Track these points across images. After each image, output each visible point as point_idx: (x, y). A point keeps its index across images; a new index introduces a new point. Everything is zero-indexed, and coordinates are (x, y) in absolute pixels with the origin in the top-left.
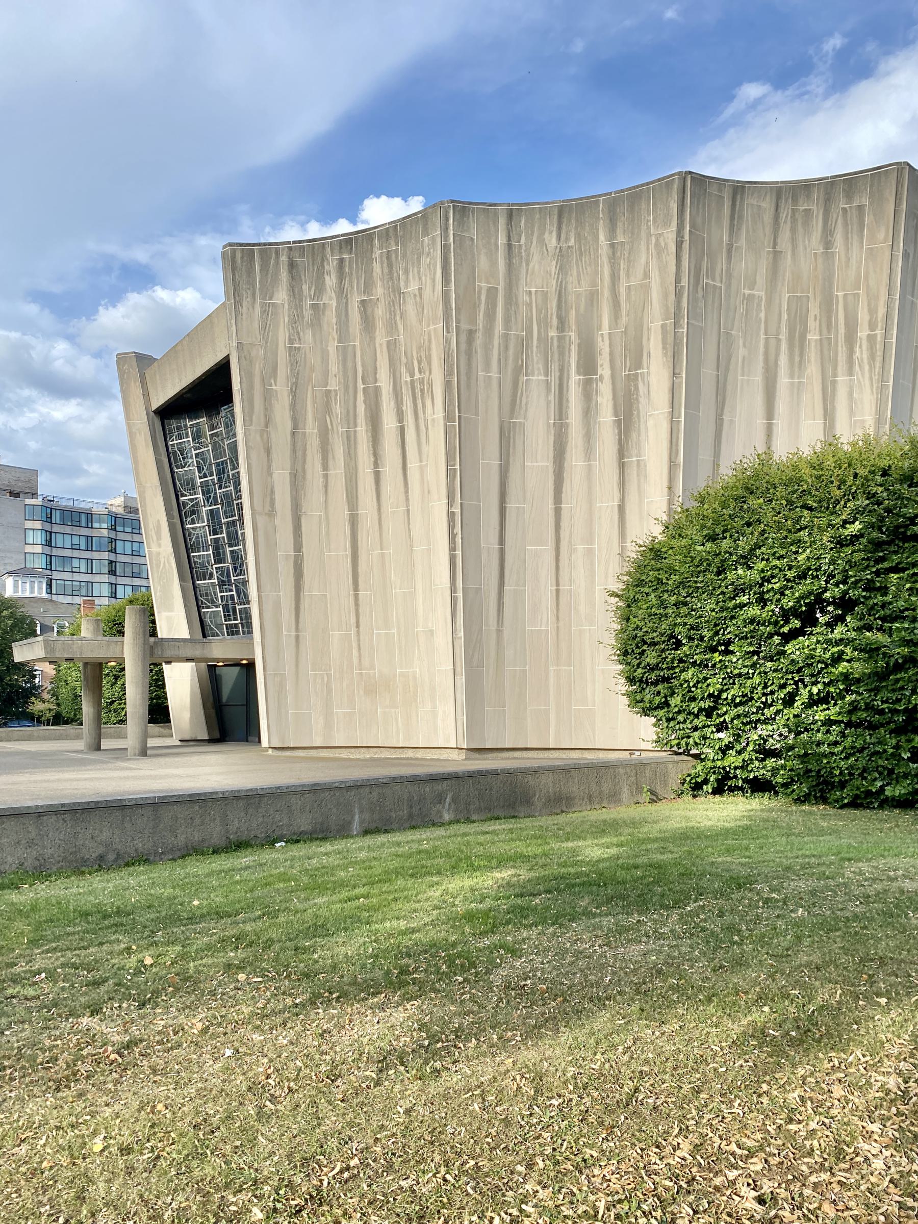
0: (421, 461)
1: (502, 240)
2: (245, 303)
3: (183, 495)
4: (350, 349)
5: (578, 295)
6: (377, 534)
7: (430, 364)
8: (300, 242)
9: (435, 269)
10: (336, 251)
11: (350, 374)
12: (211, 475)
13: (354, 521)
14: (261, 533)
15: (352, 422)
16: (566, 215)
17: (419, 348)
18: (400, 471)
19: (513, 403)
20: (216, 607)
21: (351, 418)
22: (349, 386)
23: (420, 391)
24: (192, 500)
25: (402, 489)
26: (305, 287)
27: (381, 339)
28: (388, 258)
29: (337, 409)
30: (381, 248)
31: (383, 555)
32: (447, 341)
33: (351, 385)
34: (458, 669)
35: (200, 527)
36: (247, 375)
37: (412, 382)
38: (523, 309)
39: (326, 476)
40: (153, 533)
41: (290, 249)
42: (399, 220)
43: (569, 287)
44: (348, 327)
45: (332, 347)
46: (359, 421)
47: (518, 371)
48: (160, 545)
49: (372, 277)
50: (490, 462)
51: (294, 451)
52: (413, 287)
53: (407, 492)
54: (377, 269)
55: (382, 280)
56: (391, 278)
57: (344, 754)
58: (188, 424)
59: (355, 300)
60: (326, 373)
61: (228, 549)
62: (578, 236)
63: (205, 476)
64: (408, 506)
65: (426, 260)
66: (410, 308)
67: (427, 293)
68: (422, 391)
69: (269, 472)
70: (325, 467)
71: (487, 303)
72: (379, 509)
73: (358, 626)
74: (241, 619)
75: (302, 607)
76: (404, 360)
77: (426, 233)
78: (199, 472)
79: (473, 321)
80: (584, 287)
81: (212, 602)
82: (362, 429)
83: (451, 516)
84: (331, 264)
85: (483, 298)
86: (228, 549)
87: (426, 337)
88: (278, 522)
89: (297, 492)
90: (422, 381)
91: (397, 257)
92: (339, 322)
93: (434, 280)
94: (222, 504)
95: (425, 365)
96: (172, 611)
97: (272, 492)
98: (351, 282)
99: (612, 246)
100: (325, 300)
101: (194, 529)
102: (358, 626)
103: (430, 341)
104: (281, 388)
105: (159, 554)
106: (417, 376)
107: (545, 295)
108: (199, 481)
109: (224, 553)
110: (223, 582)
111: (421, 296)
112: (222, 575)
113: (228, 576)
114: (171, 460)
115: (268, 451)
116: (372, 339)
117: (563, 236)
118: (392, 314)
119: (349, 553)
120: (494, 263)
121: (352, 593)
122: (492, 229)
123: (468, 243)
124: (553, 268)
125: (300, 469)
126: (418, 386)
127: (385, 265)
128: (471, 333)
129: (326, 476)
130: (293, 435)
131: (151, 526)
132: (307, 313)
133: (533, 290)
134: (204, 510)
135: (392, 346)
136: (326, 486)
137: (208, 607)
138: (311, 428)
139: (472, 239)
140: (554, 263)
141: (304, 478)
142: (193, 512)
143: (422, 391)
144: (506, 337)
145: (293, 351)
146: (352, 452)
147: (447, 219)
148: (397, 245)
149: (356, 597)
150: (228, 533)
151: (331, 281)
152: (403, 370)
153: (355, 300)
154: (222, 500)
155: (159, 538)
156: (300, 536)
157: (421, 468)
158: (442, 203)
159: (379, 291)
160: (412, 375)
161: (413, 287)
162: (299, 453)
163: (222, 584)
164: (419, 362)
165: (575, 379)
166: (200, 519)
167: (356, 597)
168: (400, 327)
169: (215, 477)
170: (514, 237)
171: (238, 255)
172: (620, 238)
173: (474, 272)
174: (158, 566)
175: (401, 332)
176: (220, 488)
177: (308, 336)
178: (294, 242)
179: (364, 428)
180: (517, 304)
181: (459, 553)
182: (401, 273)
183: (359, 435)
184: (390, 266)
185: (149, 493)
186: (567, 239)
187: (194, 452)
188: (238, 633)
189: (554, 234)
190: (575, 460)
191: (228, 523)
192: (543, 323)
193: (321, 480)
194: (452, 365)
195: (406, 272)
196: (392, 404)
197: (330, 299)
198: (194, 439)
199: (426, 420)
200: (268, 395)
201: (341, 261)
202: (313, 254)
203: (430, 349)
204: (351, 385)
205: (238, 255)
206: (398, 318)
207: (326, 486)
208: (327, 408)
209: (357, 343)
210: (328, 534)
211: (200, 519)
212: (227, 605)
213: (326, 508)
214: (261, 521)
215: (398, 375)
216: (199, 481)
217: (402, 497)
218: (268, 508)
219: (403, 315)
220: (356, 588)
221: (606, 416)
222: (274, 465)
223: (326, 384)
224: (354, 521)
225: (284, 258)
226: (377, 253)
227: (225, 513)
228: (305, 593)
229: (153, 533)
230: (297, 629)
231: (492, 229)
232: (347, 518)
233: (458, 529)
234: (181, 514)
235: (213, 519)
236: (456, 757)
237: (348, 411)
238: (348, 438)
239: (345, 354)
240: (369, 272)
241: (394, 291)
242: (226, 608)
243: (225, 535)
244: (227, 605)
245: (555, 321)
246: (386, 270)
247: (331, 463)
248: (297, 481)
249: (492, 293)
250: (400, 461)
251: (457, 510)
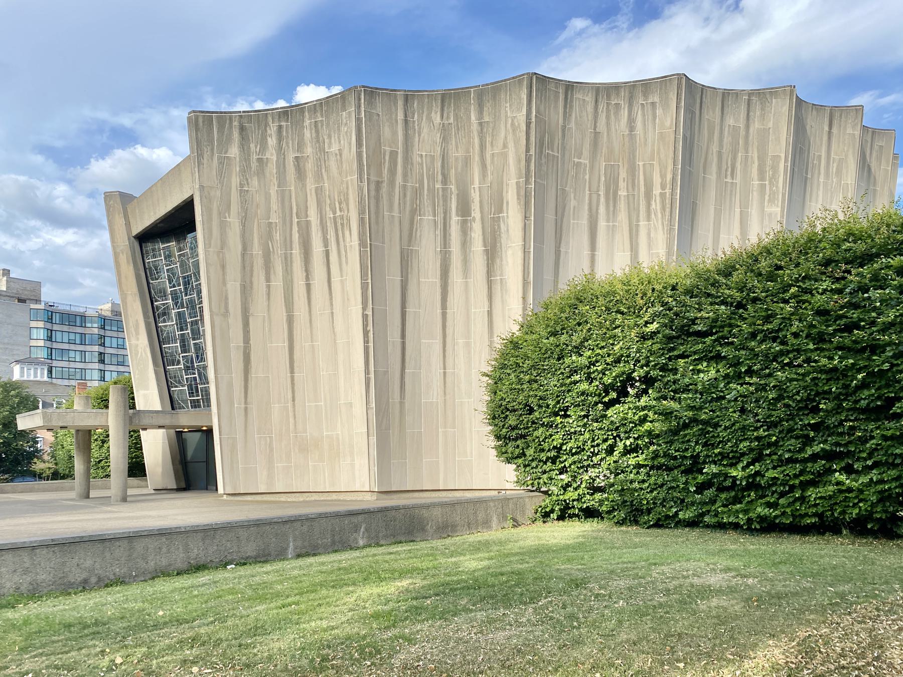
0: (342, 276)
1: (400, 116)
2: (205, 156)
3: (156, 301)
4: (287, 193)
5: (457, 159)
6: (309, 331)
7: (347, 205)
8: (248, 112)
9: (351, 136)
10: (276, 120)
11: (287, 211)
13: (290, 320)
14: (217, 329)
15: (288, 246)
16: (447, 101)
17: (339, 193)
18: (326, 284)
19: (410, 236)
20: (183, 386)
21: (287, 244)
22: (286, 221)
23: (340, 225)
24: (164, 304)
25: (327, 296)
26: (252, 146)
27: (311, 185)
28: (316, 126)
29: (277, 236)
30: (310, 118)
31: (313, 346)
32: (361, 189)
33: (288, 219)
34: (371, 432)
35: (170, 325)
36: (208, 210)
37: (335, 218)
38: (416, 168)
39: (268, 287)
40: (133, 330)
41: (241, 116)
42: (324, 99)
43: (450, 152)
44: (285, 177)
45: (273, 190)
46: (294, 246)
47: (413, 212)
48: (138, 339)
49: (303, 139)
50: (393, 278)
51: (244, 267)
52: (335, 148)
53: (331, 299)
54: (307, 134)
55: (311, 142)
56: (318, 141)
57: (283, 498)
59: (291, 156)
60: (268, 210)
61: (192, 342)
62: (456, 117)
63: (174, 286)
64: (332, 309)
65: (344, 129)
66: (333, 164)
67: (345, 152)
68: (342, 225)
69: (224, 283)
70: (268, 280)
71: (390, 162)
72: (310, 312)
73: (294, 400)
75: (249, 386)
76: (328, 202)
77: (344, 108)
78: (170, 283)
79: (380, 174)
80: (460, 154)
81: (180, 382)
82: (296, 251)
83: (365, 317)
84: (272, 129)
85: (387, 158)
86: (192, 342)
87: (345, 186)
88: (231, 320)
89: (246, 299)
90: (342, 217)
91: (322, 126)
92: (278, 172)
93: (350, 144)
94: (187, 308)
95: (344, 206)
96: (148, 389)
97: (227, 298)
98: (287, 143)
99: (481, 124)
100: (268, 155)
101: (166, 326)
102: (294, 400)
103: (347, 188)
104: (234, 220)
105: (137, 345)
106: (338, 213)
107: (433, 157)
109: (189, 345)
110: (188, 367)
111: (341, 155)
113: (192, 362)
114: (148, 273)
115: (223, 267)
116: (304, 186)
117: (445, 115)
118: (319, 167)
119: (286, 344)
120: (395, 133)
121: (289, 375)
122: (393, 108)
123: (375, 117)
124: (438, 138)
125: (248, 282)
126: (339, 221)
127: (313, 131)
128: (378, 184)
129: (268, 287)
130: (243, 255)
131: (131, 324)
132: (254, 165)
133: (424, 154)
134: (173, 312)
135: (319, 191)
136: (269, 294)
137: (176, 387)
138: (257, 250)
139: (378, 115)
140: (439, 135)
141: (251, 288)
142: (164, 314)
143: (342, 225)
144: (405, 187)
145: (243, 193)
146: (289, 268)
147: (360, 99)
148: (322, 116)
149: (292, 378)
150: (192, 330)
151: (272, 141)
152: (328, 209)
153: (291, 156)
155: (137, 333)
156: (248, 332)
157: (341, 281)
158: (356, 87)
159: (309, 150)
160: (335, 213)
161: (335, 148)
162: (248, 269)
163: (187, 368)
164: (340, 203)
165: (455, 219)
166: (170, 319)
167: (292, 378)
168: (325, 177)
170: (409, 114)
171: (200, 120)
172: (486, 119)
173: (380, 140)
174: (137, 354)
175: (326, 181)
176: (186, 295)
177: (255, 182)
178: (244, 112)
179: (298, 251)
180: (412, 164)
181: (371, 344)
182: (325, 137)
183: (294, 256)
184: (317, 132)
185: (130, 299)
186: (448, 118)
188: (199, 406)
189: (439, 114)
190: (456, 276)
191: (192, 322)
192: (432, 178)
193: (265, 289)
194: (364, 207)
195: (330, 137)
196: (320, 234)
197: (271, 155)
198: (165, 258)
199: (345, 246)
200: (223, 226)
201: (280, 127)
202: (258, 121)
203: (348, 194)
204: (288, 219)
205: (200, 120)
206: (323, 170)
207: (269, 294)
208: (270, 236)
209: (293, 188)
210: (270, 330)
211: (170, 319)
212: (191, 385)
213: (268, 310)
214: (217, 320)
215: (324, 213)
216: (169, 290)
217: (328, 303)
218: (223, 310)
220: (292, 371)
222: (228, 278)
223: (269, 218)
224: (290, 320)
225: (236, 123)
226: (307, 122)
227: (190, 314)
228: (253, 375)
229: (133, 330)
230: (246, 403)
231: (393, 108)
232: (285, 318)
233: (370, 328)
234: (156, 315)
235: (180, 319)
236: (369, 498)
237: (286, 239)
238: (286, 258)
239: (283, 196)
241: (320, 151)
244: (191, 385)
245: (440, 177)
246: (314, 135)
247: (272, 277)
248: (246, 290)
249: (394, 154)
250: (326, 276)
251: (370, 313)
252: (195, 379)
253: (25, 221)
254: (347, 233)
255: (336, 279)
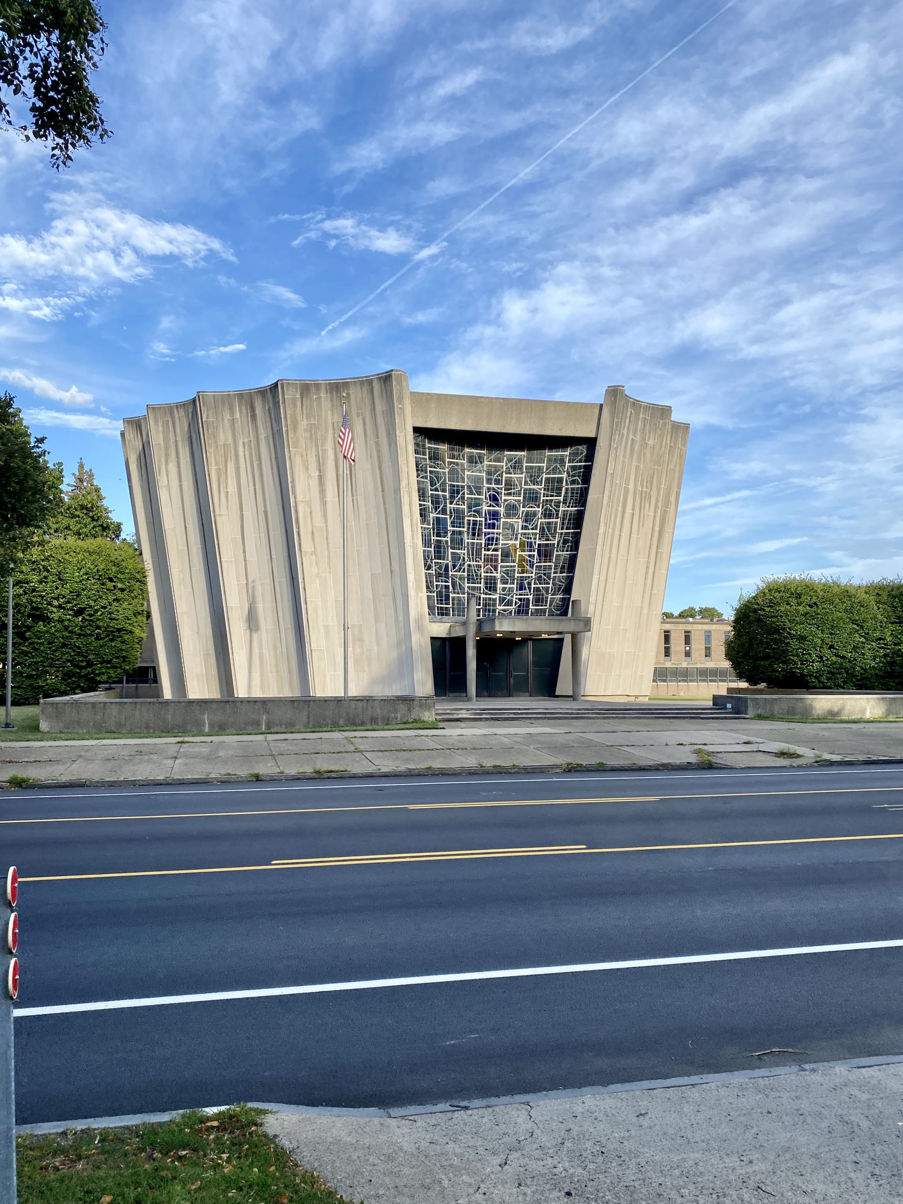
7: (651, 485)
12: (444, 490)
23: (645, 497)
27: (634, 463)
52: (651, 442)
58: (427, 445)
63: (436, 490)
67: (657, 448)
74: (453, 604)
86: (450, 551)
87: (651, 471)
108: (430, 492)
109: (444, 552)
112: (440, 568)
118: (641, 451)
135: (637, 467)
153: (631, 437)
154: (451, 512)
159: (638, 436)
161: (651, 442)
163: (439, 575)
169: (447, 494)
187: (429, 469)
188: (447, 614)
191: (453, 531)
195: (650, 433)
203: (653, 477)
212: (441, 592)
219: (645, 454)
221: (657, 528)
240: (637, 424)
242: (440, 594)
243: (449, 539)
244: (441, 592)
252: (447, 587)
253: (283, 354)
254: (647, 505)
255: (634, 536)
